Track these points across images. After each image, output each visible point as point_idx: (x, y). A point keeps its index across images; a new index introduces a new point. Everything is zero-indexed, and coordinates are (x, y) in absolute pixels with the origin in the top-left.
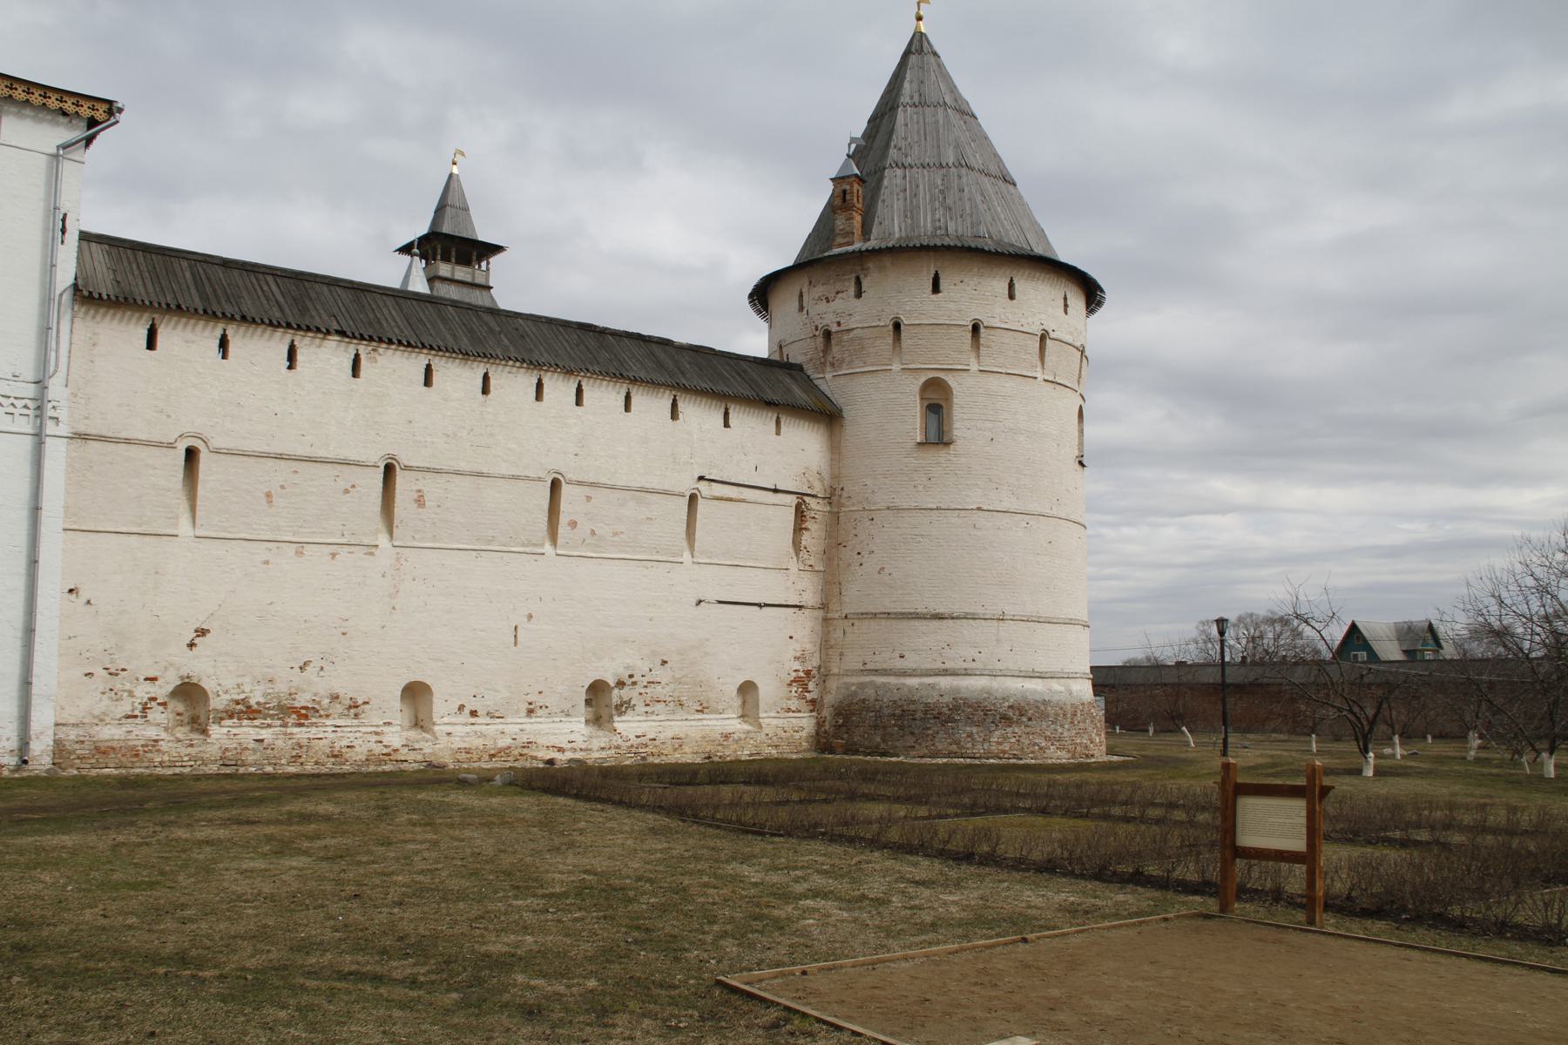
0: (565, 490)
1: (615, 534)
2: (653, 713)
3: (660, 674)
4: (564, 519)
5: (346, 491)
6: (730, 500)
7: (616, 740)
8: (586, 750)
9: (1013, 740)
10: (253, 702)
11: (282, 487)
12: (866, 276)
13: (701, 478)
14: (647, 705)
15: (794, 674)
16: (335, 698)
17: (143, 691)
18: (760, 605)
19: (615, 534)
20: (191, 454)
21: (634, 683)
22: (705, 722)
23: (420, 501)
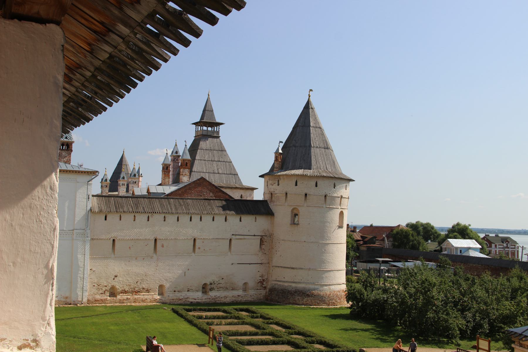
0: (197, 241)
1: (210, 250)
2: (219, 290)
3: (221, 281)
4: (197, 247)
5: (146, 245)
6: (241, 239)
7: (209, 297)
8: (201, 299)
9: (310, 301)
10: (126, 290)
11: (133, 246)
12: (280, 180)
13: (233, 235)
14: (218, 289)
15: (259, 280)
16: (143, 289)
17: (104, 289)
18: (249, 264)
19: (210, 250)
20: (114, 240)
21: (215, 284)
22: (233, 293)
23: (163, 246)
